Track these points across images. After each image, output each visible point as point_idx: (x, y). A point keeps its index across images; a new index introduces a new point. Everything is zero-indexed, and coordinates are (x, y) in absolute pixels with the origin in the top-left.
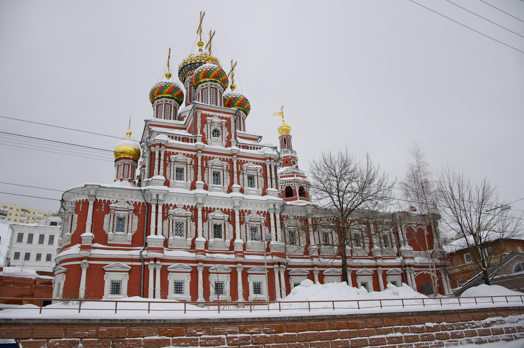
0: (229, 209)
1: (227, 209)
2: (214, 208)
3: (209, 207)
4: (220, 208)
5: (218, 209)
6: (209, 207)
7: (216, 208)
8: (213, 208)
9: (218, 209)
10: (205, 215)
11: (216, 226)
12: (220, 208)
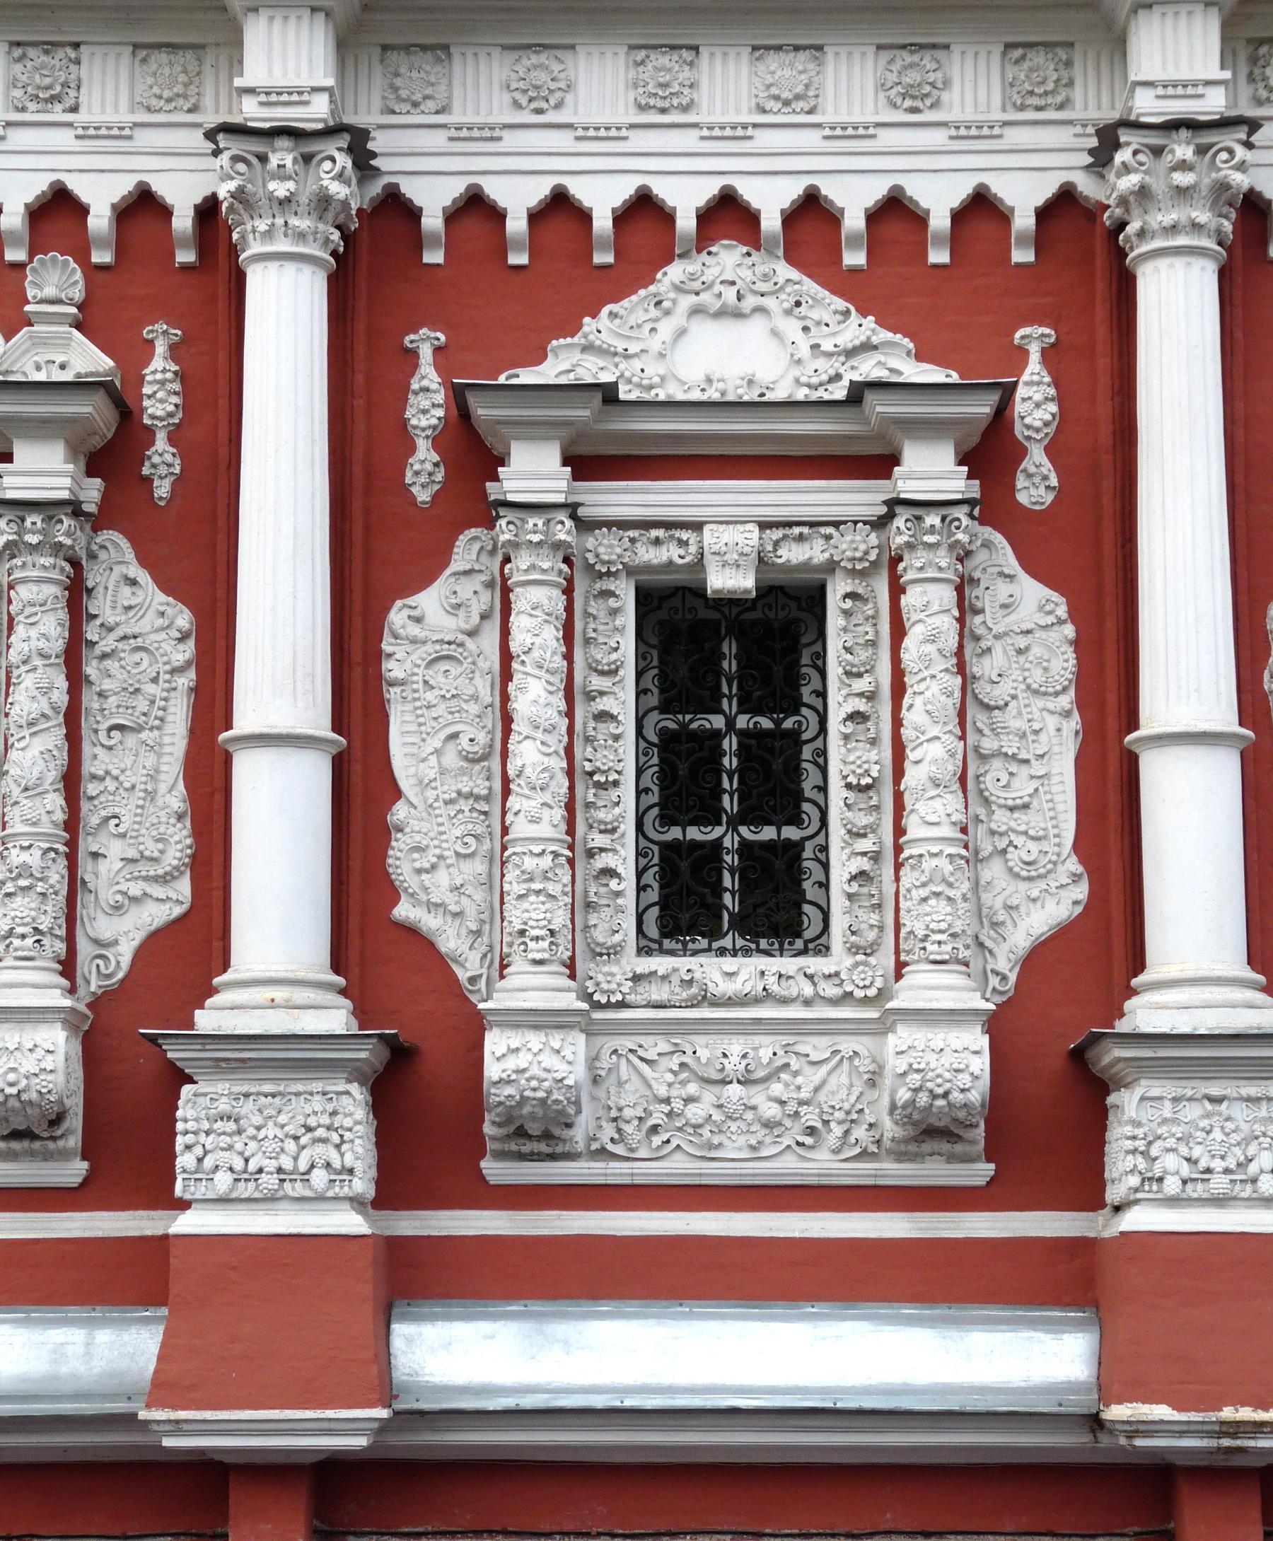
0: (981, 209)
1: (939, 199)
2: (644, 210)
3: (517, 199)
4: (771, 200)
5: (728, 216)
6: (517, 199)
7: (686, 199)
8: (602, 199)
9: (728, 216)
10: (426, 407)
11: (680, 626)
12: (771, 200)
